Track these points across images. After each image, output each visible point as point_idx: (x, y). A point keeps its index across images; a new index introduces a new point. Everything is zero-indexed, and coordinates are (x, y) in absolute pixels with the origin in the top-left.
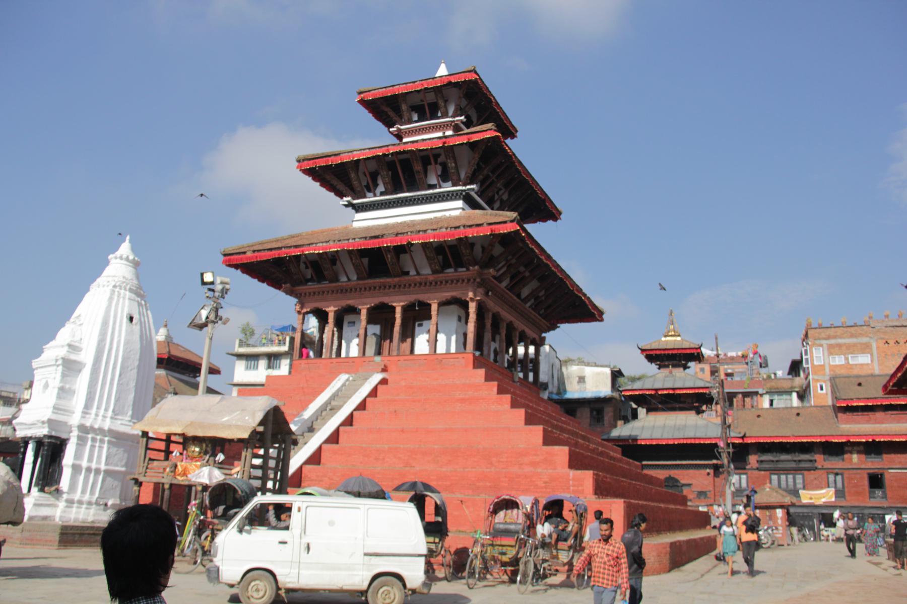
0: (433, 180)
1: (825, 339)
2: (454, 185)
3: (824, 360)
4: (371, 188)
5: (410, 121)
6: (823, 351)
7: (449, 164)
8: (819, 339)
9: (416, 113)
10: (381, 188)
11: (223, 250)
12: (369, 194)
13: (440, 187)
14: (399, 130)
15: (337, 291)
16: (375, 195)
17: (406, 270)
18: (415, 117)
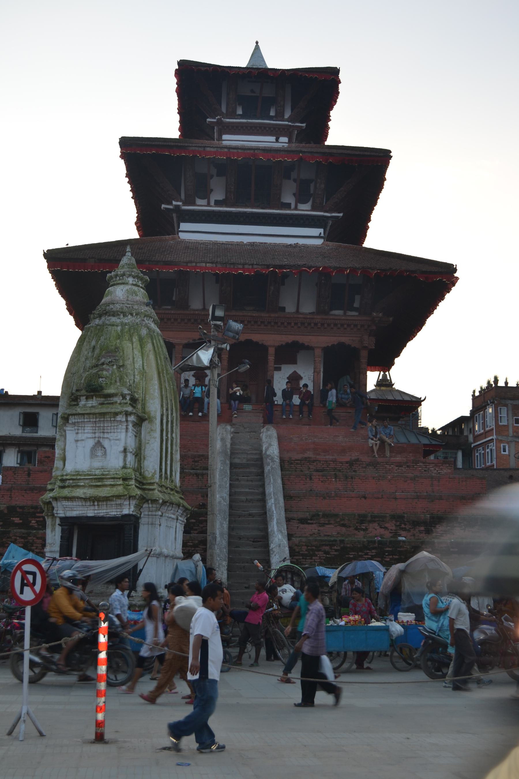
0: (288, 198)
1: (511, 399)
2: (313, 209)
3: (508, 420)
4: (205, 194)
5: (234, 115)
6: (507, 411)
7: (318, 185)
8: (505, 399)
9: (239, 104)
10: (218, 195)
11: (45, 252)
12: (204, 202)
13: (296, 209)
14: (219, 122)
15: (189, 320)
16: (209, 205)
17: (281, 305)
18: (240, 111)
